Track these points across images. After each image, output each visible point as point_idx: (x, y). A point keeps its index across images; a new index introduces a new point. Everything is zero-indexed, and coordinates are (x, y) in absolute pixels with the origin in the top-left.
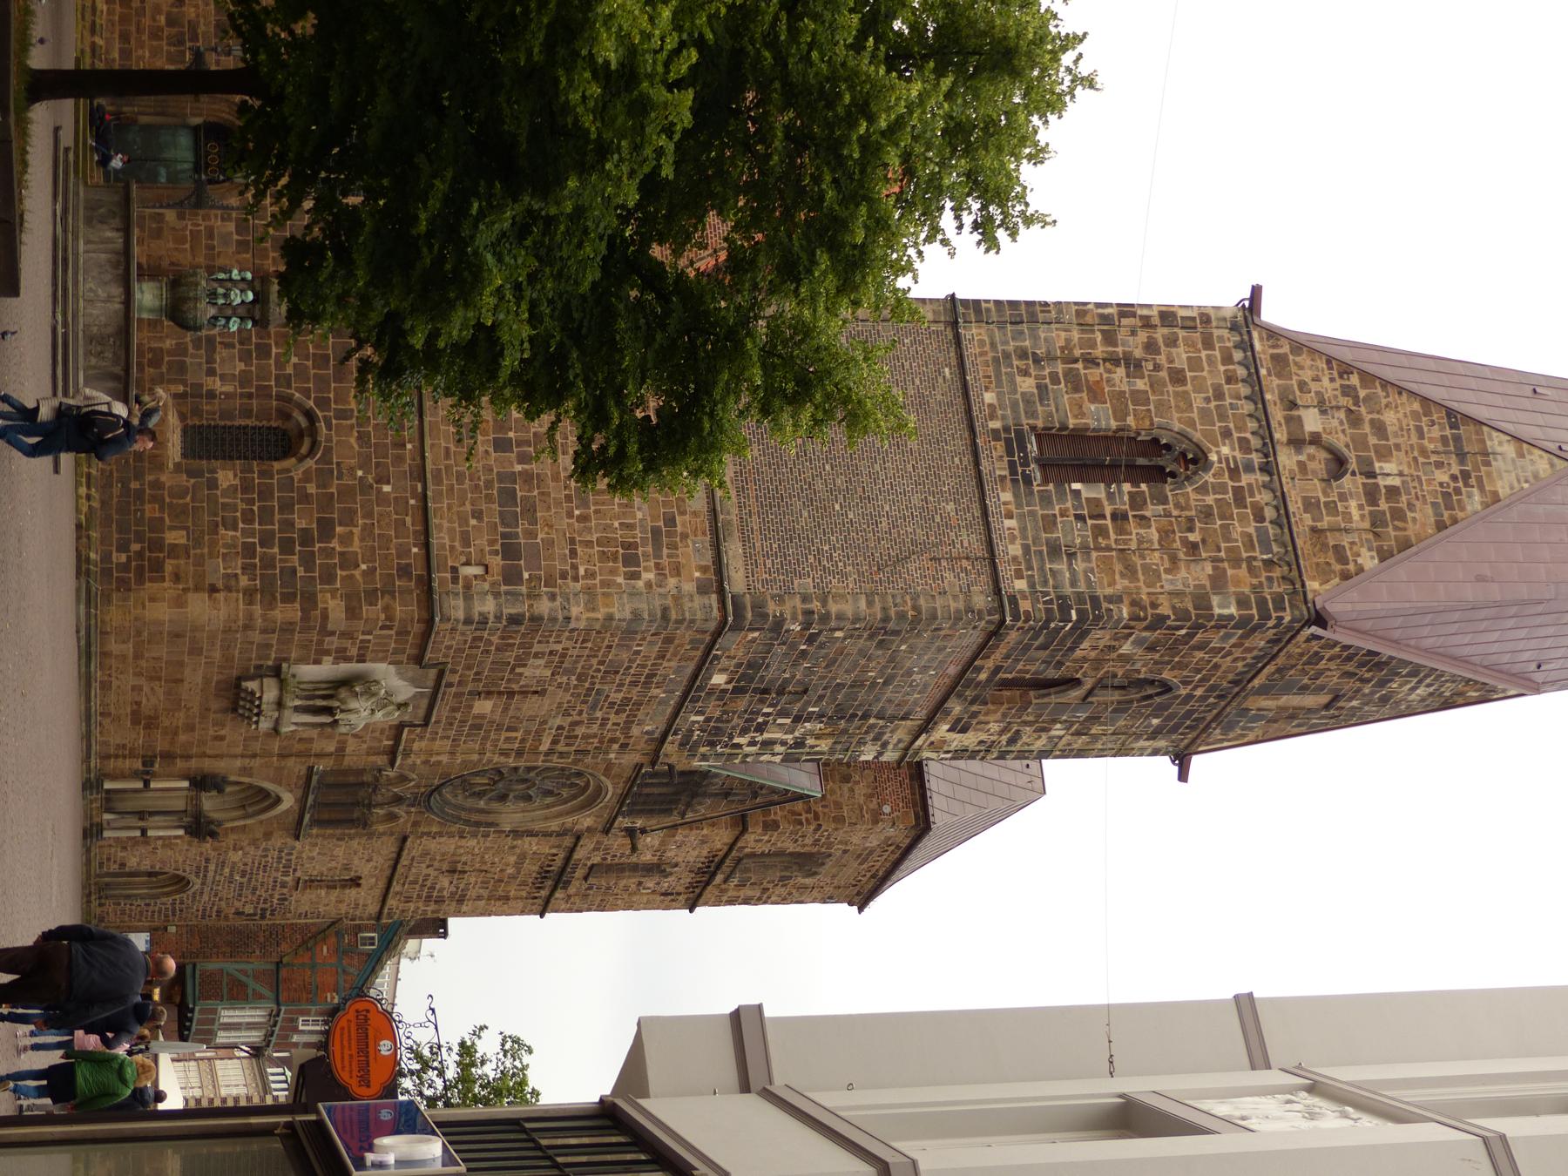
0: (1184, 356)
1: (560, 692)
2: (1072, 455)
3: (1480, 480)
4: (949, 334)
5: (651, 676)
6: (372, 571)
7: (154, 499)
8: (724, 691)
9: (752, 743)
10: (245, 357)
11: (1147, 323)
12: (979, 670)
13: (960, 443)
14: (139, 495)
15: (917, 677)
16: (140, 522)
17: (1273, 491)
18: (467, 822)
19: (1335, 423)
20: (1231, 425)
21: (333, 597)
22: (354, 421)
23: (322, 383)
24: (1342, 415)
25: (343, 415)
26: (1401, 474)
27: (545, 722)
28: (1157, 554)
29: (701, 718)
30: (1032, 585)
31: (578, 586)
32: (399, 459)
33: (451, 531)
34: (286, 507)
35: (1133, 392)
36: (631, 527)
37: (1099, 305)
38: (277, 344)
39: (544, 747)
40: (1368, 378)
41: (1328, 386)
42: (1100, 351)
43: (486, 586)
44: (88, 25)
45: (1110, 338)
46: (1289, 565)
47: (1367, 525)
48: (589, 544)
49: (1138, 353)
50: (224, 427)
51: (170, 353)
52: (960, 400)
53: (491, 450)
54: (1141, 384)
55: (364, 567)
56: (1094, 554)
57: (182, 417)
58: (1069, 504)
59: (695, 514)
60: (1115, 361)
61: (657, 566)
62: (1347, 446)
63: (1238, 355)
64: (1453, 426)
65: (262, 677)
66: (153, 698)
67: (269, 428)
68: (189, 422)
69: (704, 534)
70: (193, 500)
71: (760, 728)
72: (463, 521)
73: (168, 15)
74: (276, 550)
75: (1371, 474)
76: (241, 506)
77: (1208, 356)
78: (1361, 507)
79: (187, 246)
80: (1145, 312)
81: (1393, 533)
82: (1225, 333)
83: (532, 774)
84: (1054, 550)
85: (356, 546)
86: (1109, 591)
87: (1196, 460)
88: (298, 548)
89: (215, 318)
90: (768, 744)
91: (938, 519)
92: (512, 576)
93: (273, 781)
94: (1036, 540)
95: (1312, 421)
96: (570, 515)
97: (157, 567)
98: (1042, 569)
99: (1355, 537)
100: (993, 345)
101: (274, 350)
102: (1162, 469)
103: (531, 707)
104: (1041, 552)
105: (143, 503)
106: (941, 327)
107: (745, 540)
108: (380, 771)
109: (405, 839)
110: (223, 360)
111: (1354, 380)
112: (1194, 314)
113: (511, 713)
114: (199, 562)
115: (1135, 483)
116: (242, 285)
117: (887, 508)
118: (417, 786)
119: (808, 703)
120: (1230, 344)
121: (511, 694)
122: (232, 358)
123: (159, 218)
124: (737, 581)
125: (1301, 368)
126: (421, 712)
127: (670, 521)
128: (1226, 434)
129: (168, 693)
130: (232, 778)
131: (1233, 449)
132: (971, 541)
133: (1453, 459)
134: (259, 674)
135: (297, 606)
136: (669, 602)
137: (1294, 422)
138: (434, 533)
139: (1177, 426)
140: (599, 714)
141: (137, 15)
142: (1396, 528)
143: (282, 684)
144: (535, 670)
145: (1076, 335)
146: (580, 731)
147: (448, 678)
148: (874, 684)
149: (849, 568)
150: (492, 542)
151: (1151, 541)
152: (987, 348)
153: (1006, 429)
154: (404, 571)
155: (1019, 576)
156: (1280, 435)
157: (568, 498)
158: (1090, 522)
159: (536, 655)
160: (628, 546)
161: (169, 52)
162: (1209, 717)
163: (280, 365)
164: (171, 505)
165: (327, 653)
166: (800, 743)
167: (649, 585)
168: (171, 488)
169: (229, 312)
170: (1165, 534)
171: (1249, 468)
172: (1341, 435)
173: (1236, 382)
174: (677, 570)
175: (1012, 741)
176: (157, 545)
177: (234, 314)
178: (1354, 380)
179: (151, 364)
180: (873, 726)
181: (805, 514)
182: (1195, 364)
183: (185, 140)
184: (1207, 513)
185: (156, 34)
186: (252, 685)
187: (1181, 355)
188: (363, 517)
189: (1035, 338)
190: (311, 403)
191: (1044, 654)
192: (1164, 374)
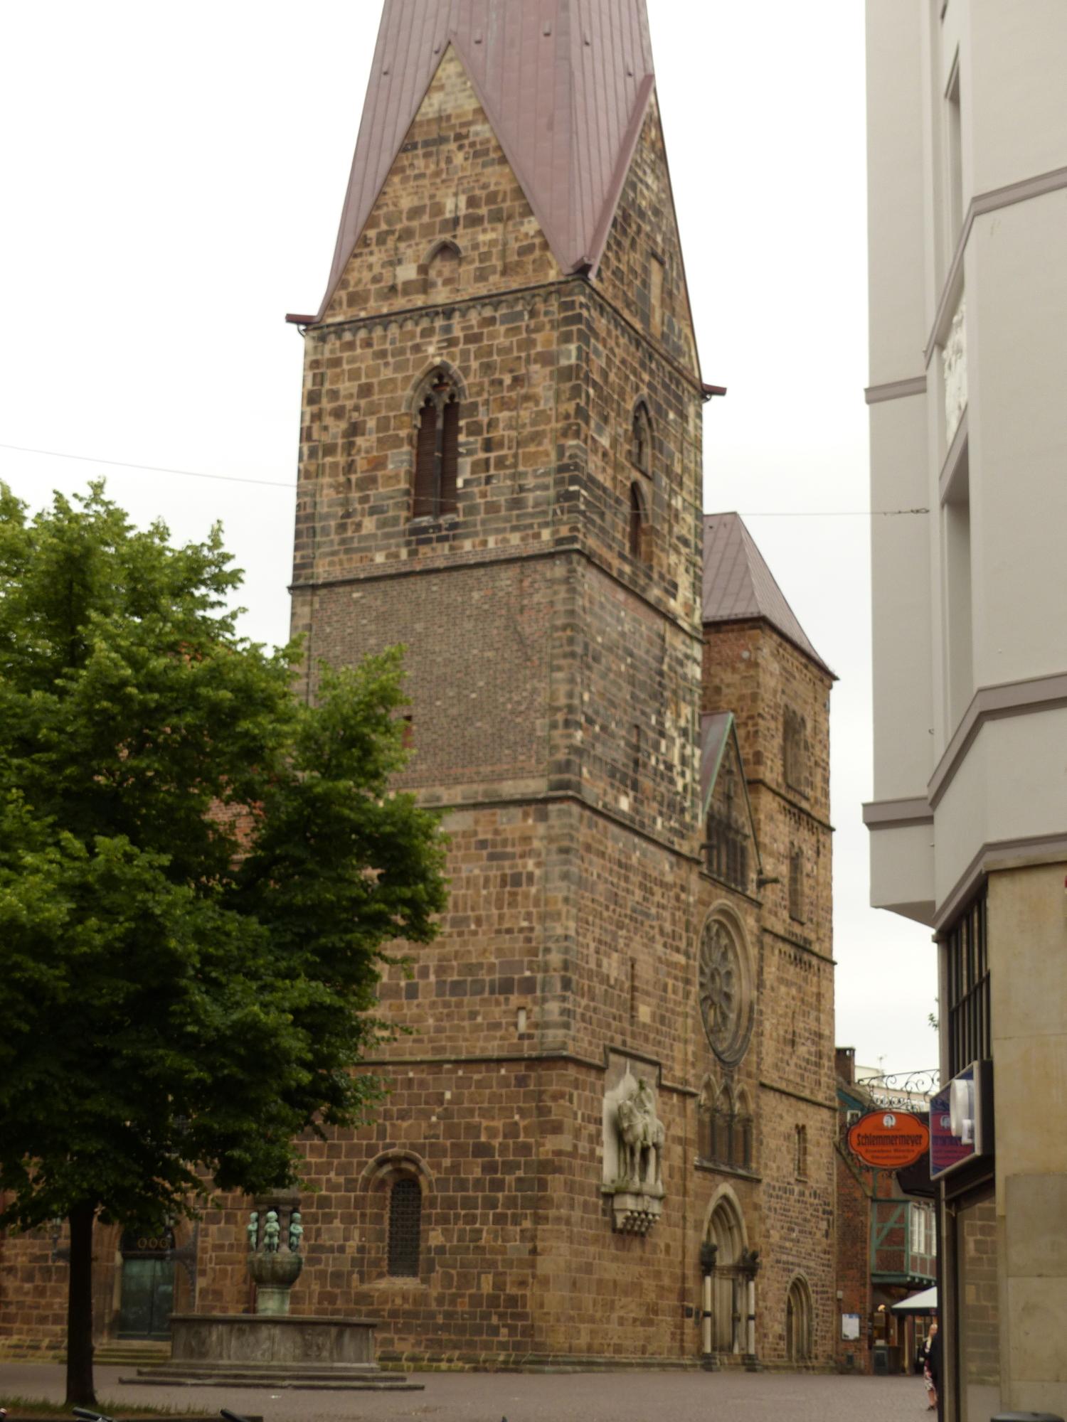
0: (347, 384)
1: (633, 945)
2: (433, 483)
3: (463, 125)
4: (323, 592)
5: (620, 864)
6: (521, 1111)
7: (453, 1302)
8: (635, 799)
9: (683, 774)
10: (329, 1218)
11: (317, 417)
12: (621, 572)
13: (420, 584)
14: (449, 1315)
15: (627, 627)
16: (473, 1316)
17: (469, 308)
18: (749, 1029)
19: (410, 252)
20: (410, 344)
21: (543, 1145)
22: (388, 1123)
23: (353, 1151)
24: (402, 245)
25: (382, 1134)
26: (456, 195)
27: (660, 959)
28: (522, 413)
29: (659, 821)
30: (546, 525)
31: (538, 927)
32: (422, 1084)
33: (487, 1039)
34: (462, 1185)
35: (379, 429)
36: (487, 880)
37: (301, 459)
39: (681, 959)
40: (371, 222)
41: (377, 257)
42: (340, 459)
43: (536, 1009)
44: (31, 1352)
45: (330, 450)
46: (534, 296)
47: (500, 226)
48: (501, 917)
49: (343, 425)
50: (391, 1238)
51: (323, 1286)
52: (382, 585)
53: (415, 1002)
54: (371, 423)
55: (517, 1117)
56: (521, 468)
57: (380, 1275)
58: (476, 490)
59: (477, 822)
60: (350, 446)
61: (522, 856)
62: (430, 241)
63: (347, 336)
64: (415, 146)
65: (613, 1210)
66: (630, 1307)
67: (392, 1198)
68: (385, 1269)
69: (494, 815)
70: (454, 1267)
71: (670, 767)
72: (477, 1028)
74: (500, 1195)
75: (456, 221)
76: (461, 1225)
77: (349, 362)
78: (484, 231)
79: (229, 1268)
80: (308, 418)
81: (508, 203)
82: (328, 347)
83: (707, 970)
84: (516, 504)
85: (499, 1124)
86: (553, 456)
87: (440, 375)
88: (499, 1175)
89: (291, 1246)
90: (684, 761)
91: (486, 607)
92: (528, 987)
93: (707, 1201)
94: (507, 520)
95: (408, 272)
96: (475, 933)
97: (512, 1301)
98: (532, 515)
99: (511, 237)
100: (334, 553)
101: (324, 1193)
102: (447, 407)
103: (645, 971)
104: (518, 516)
105: (456, 1313)
106: (316, 599)
107: (501, 778)
108: (700, 1106)
109: (763, 1085)
110: (331, 1239)
111: (372, 233)
112: (310, 374)
113: (650, 989)
114: (509, 1264)
115: (459, 430)
116: (262, 1222)
117: (475, 652)
118: (715, 1073)
119: (648, 724)
120: (338, 344)
121: (634, 989)
122: (329, 1230)
123: (204, 1292)
124: (536, 786)
125: (360, 281)
126: (648, 1068)
127: (483, 844)
128: (417, 348)
129: (626, 1294)
130: (704, 1238)
131: (430, 343)
132: (506, 578)
133: (445, 148)
134: (610, 1212)
135: (550, 1177)
136: (554, 847)
137: (408, 288)
138: (488, 1054)
139: (409, 392)
140: (653, 911)
142: (504, 200)
143: (620, 1192)
144: (613, 967)
145: (326, 480)
146: (668, 927)
147: (618, 1044)
148: (632, 666)
149: (528, 686)
150: (498, 1003)
151: (511, 418)
152: (336, 559)
153: (408, 543)
154: (522, 1081)
155: (537, 536)
156: (419, 301)
157: (460, 934)
158: (492, 472)
159: (599, 965)
160: (504, 883)
161: (57, 1281)
162: (668, 368)
163: (335, 1188)
164: (459, 1288)
165: (592, 1152)
166: (684, 732)
167: (538, 865)
168: (443, 1287)
169: (286, 1233)
170: (504, 405)
171: (447, 329)
172: (421, 247)
173: (371, 338)
174: (526, 839)
175: (686, 543)
176: (493, 1300)
177: (288, 1228)
178: (372, 233)
180: (670, 668)
181: (479, 724)
182: (354, 375)
183: (135, 1268)
184: (487, 368)
185: (41, 1292)
186: (620, 1219)
187: (347, 387)
188: (473, 1116)
189: (327, 516)
190: (371, 1161)
191: (609, 516)
192: (363, 402)
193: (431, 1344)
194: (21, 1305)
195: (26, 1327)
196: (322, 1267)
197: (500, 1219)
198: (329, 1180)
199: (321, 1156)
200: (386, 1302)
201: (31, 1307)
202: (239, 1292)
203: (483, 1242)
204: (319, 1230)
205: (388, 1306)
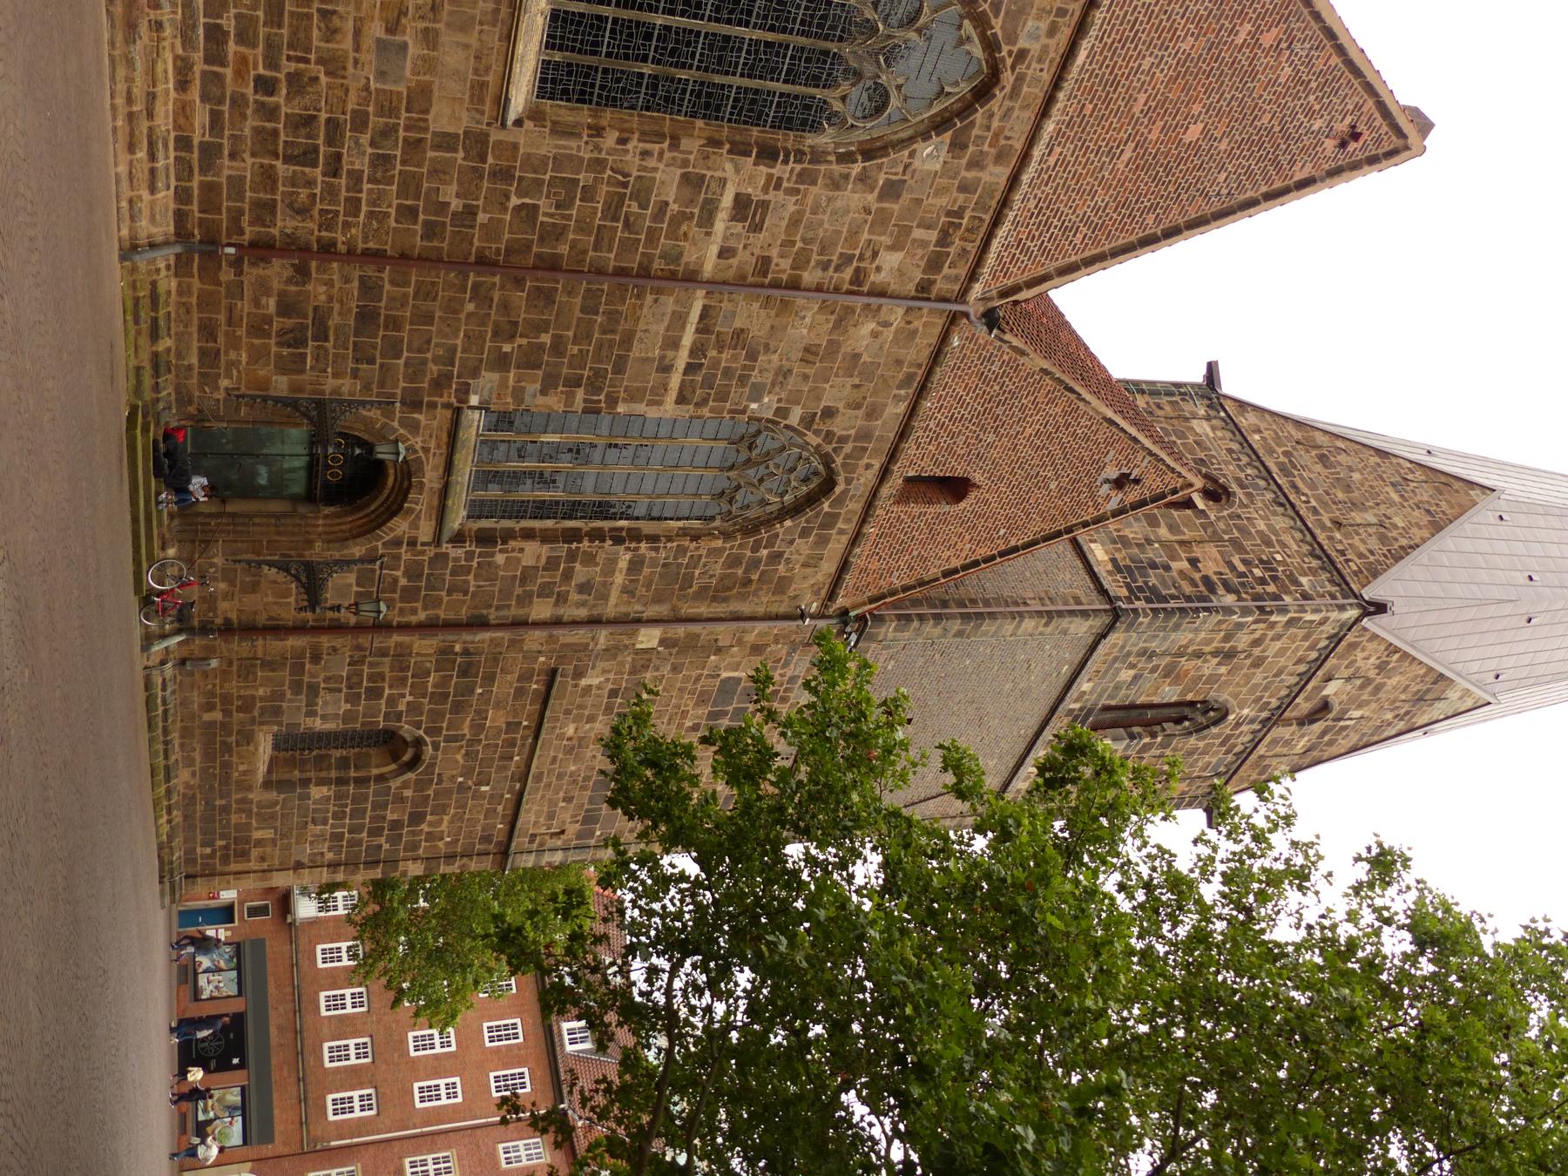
10: (353, 699)
23: (436, 715)
38: (391, 687)
44: (145, 326)
51: (262, 699)
73: (282, 295)
74: (365, 835)
76: (331, 808)
85: (444, 827)
97: (244, 855)
101: (387, 691)
105: (229, 813)
110: (326, 703)
114: (288, 847)
141: (230, 295)
161: (279, 356)
163: (392, 701)
179: (239, 709)
185: (259, 328)
190: (421, 732)
193: (189, 801)
194: (236, 290)
195: (194, 300)
196: (289, 695)
197: (340, 837)
198: (403, 696)
199: (434, 686)
200: (240, 756)
201: (230, 310)
202: (255, 613)
203: (311, 827)
204: (340, 691)
205: (235, 759)
